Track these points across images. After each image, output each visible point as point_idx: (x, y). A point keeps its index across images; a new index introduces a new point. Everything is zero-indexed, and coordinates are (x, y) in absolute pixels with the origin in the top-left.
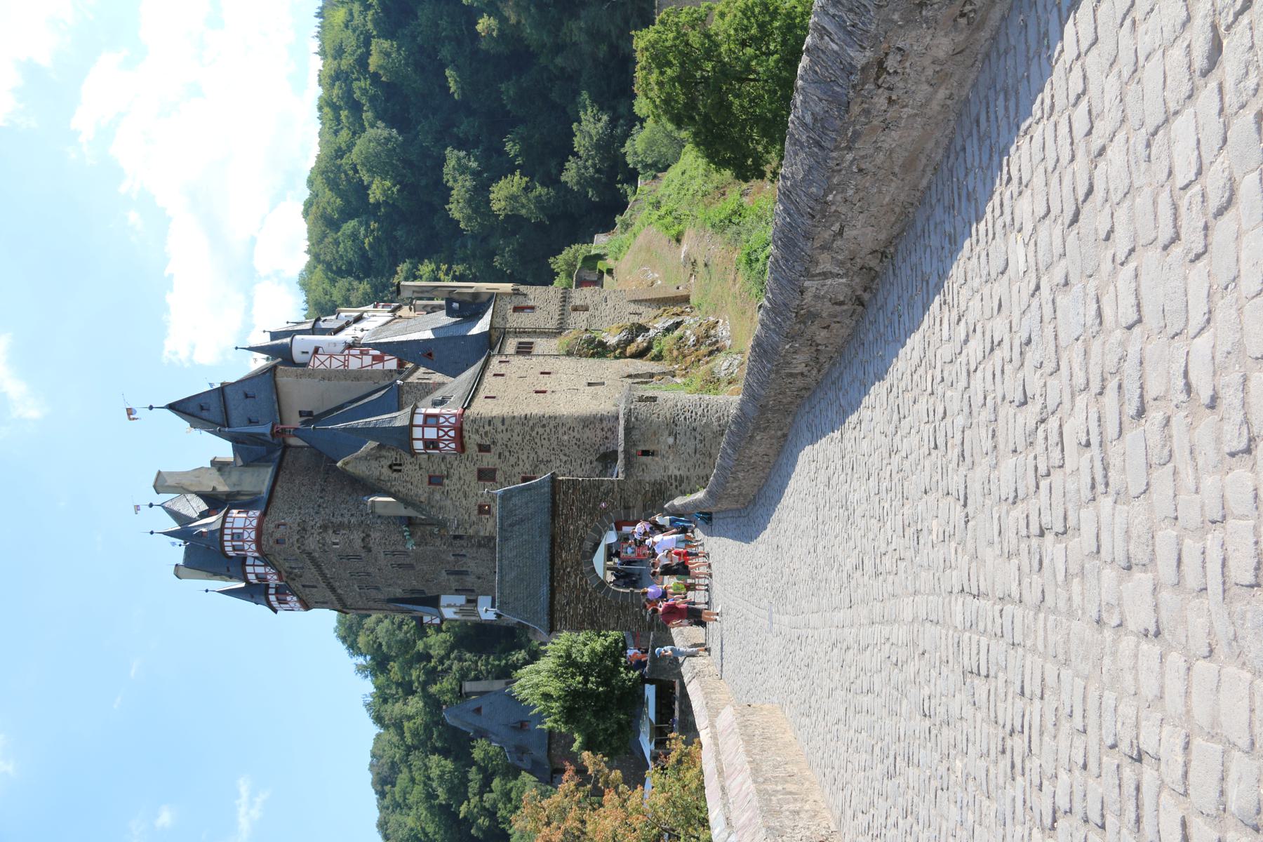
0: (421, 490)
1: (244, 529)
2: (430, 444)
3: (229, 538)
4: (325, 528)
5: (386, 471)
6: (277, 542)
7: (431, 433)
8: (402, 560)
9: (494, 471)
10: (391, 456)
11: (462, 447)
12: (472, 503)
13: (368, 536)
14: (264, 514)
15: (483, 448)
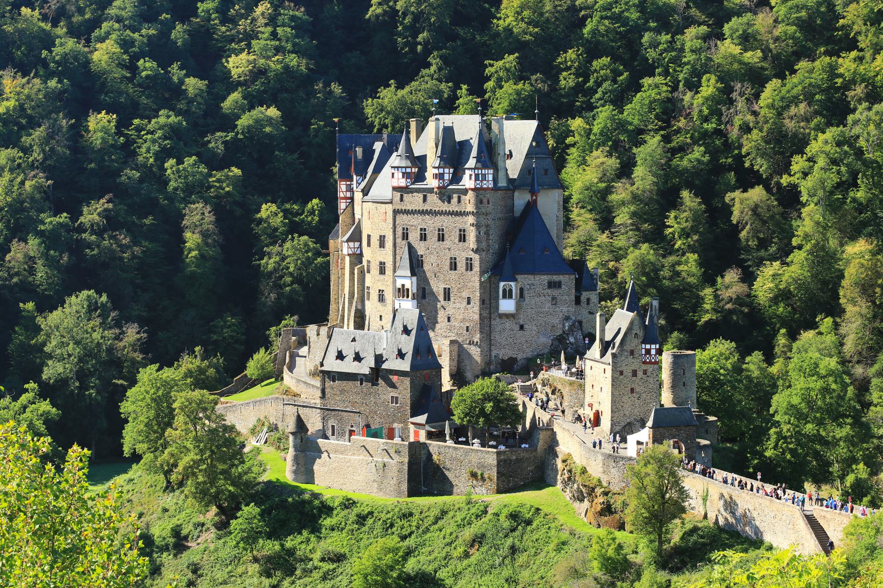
0: (628, 347)
1: (488, 181)
2: (648, 352)
3: (483, 172)
4: (487, 226)
5: (635, 332)
6: (481, 202)
7: (653, 352)
8: (461, 265)
9: (636, 376)
10: (641, 333)
11: (645, 363)
12: (623, 368)
13: (484, 251)
14: (492, 189)
15: (645, 372)
